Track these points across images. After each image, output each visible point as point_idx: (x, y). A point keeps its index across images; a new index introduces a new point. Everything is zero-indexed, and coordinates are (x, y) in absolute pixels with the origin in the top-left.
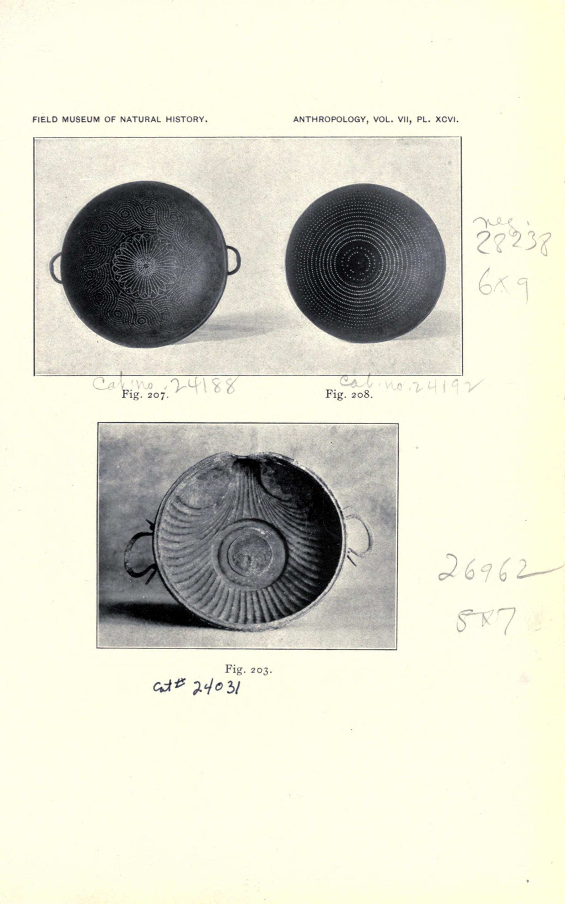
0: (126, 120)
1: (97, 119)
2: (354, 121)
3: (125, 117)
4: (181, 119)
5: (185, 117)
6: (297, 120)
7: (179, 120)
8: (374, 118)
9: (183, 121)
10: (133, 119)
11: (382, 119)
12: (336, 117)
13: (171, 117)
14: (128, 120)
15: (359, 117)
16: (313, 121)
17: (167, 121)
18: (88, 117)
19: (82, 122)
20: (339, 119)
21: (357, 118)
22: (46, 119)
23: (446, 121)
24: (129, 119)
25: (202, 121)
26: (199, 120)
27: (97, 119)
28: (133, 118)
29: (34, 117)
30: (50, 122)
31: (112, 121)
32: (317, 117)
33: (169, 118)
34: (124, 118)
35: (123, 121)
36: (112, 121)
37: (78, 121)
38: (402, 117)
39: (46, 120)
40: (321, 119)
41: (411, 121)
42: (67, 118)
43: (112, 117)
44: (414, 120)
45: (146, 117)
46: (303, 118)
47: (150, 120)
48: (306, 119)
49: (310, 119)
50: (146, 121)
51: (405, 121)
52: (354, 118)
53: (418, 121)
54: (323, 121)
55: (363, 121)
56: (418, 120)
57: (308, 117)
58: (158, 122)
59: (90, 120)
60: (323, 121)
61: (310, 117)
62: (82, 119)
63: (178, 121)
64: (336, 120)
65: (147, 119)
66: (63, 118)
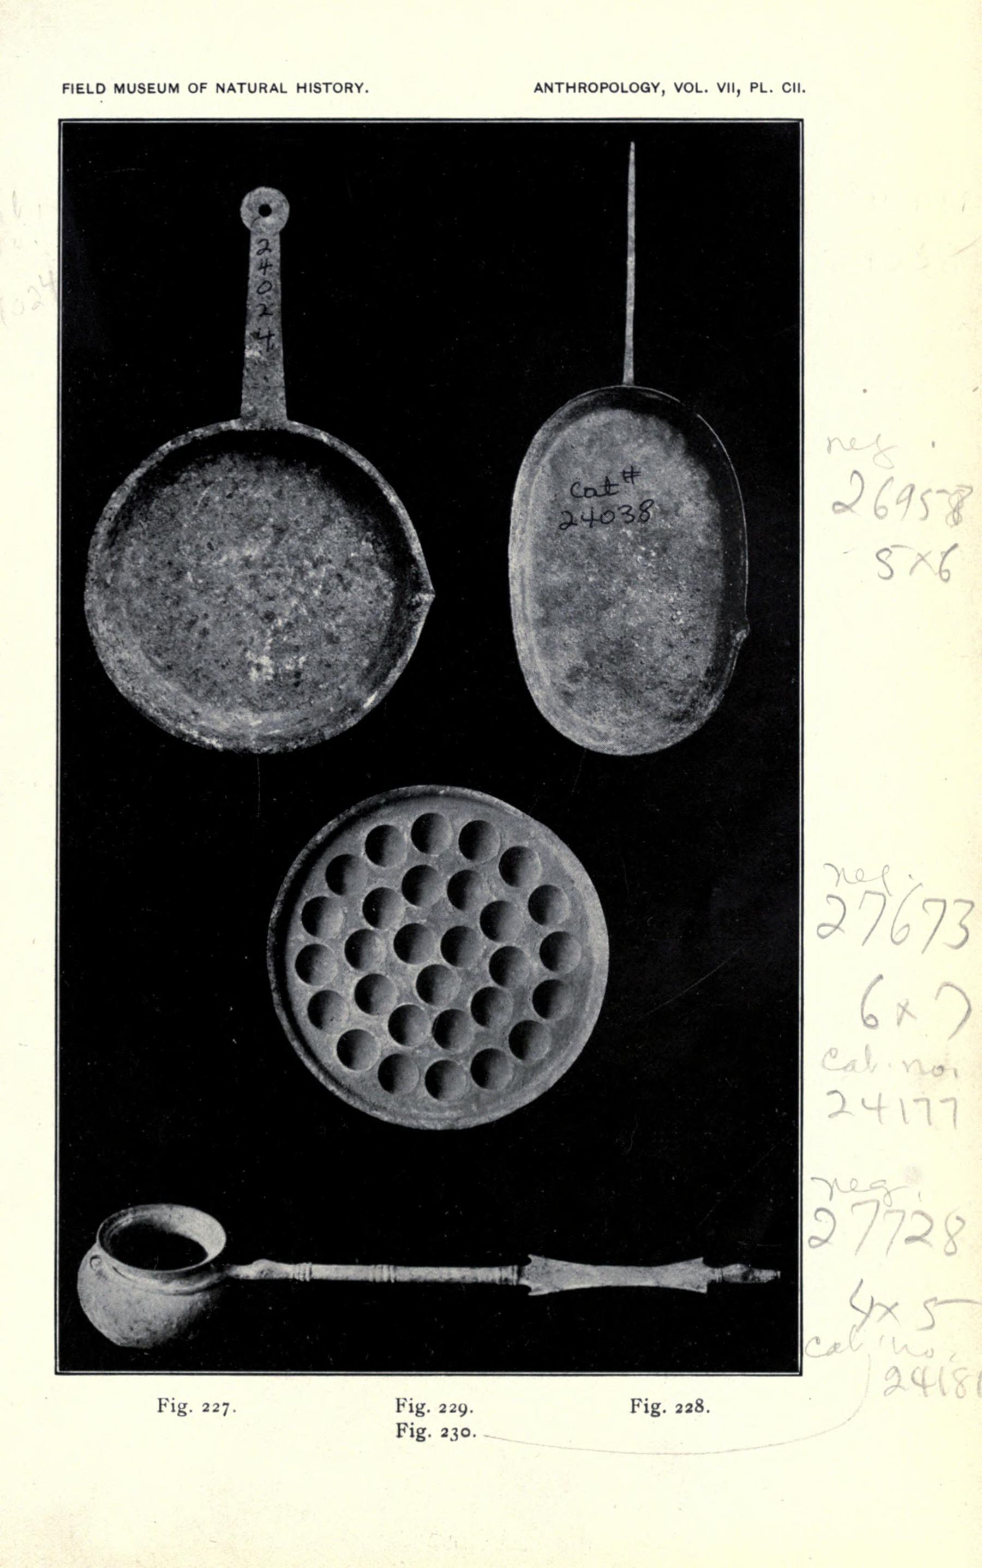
0: (226, 89)
1: (175, 88)
2: (640, 90)
3: (224, 85)
4: (323, 87)
5: (331, 84)
6: (541, 89)
7: (320, 89)
8: (676, 85)
9: (327, 91)
10: (237, 88)
11: (689, 88)
12: (609, 84)
13: (305, 85)
14: (229, 89)
15: (648, 84)
16: (567, 91)
17: (298, 91)
18: (159, 85)
19: (149, 92)
20: (614, 88)
21: (645, 86)
22: (85, 87)
23: (790, 90)
24: (232, 88)
25: (359, 91)
26: (355, 88)
27: (175, 88)
28: (239, 86)
29: (64, 85)
30: (92, 93)
31: (201, 91)
32: (575, 84)
33: (302, 85)
34: (222, 86)
35: (220, 90)
36: (201, 91)
37: (142, 90)
38: (725, 84)
39: (85, 90)
40: (583, 87)
41: (739, 91)
42: (123, 86)
43: (202, 84)
44: (745, 89)
45: (261, 84)
46: (550, 85)
47: (268, 89)
48: (556, 87)
49: (563, 87)
50: (260, 91)
51: (729, 91)
52: (640, 85)
53: (752, 91)
54: (585, 91)
55: (655, 91)
56: (752, 88)
57: (559, 84)
58: (282, 92)
59: (162, 89)
60: (585, 91)
61: (563, 83)
62: (149, 88)
63: (317, 90)
64: (608, 89)
65: (263, 87)
66: (116, 86)
